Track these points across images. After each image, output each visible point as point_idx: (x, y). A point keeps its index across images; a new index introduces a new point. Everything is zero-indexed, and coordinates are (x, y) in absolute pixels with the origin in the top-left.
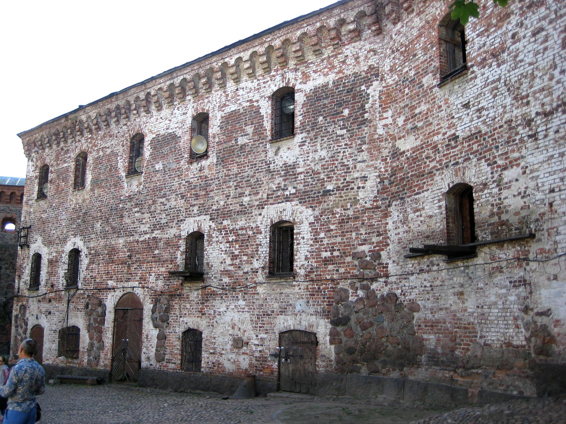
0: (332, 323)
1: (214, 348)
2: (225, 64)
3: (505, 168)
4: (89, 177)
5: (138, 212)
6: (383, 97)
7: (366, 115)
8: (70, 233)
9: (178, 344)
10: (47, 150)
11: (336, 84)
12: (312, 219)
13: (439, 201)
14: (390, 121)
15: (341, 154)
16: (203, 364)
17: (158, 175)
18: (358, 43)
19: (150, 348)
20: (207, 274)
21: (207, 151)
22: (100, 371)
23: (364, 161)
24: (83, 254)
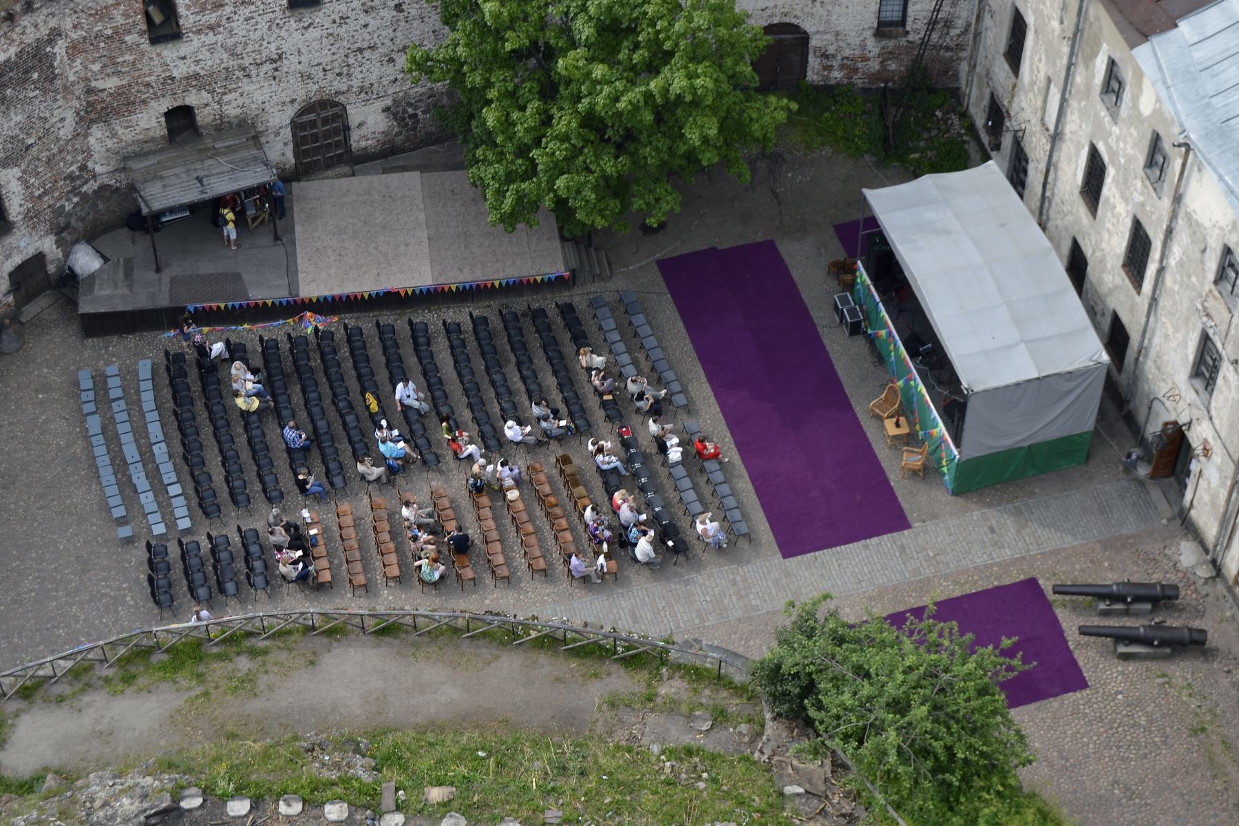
3: (225, 94)
7: (57, 72)
11: (19, 55)
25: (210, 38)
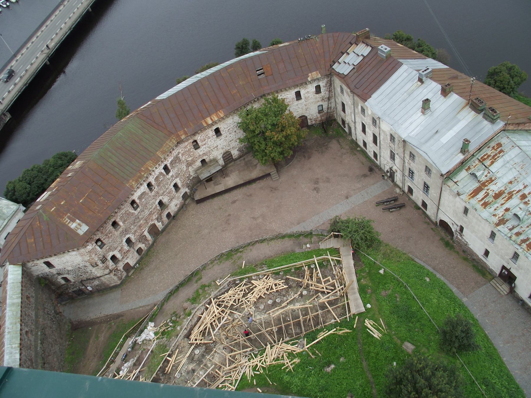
25: (205, 146)
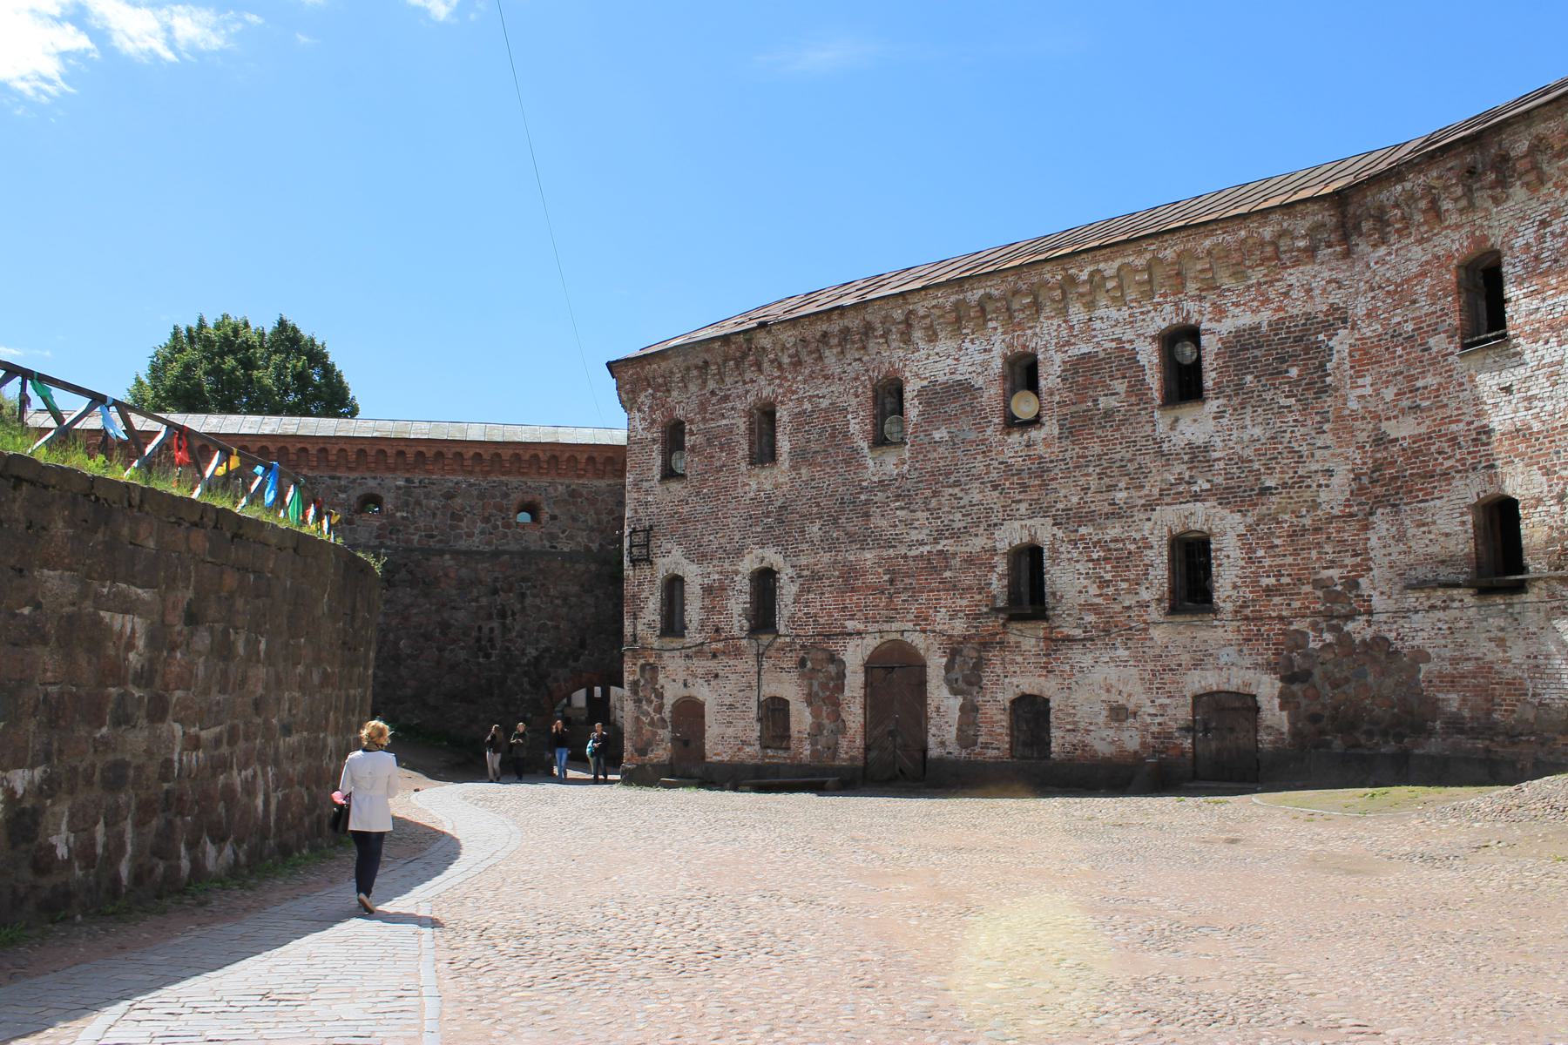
0: (1282, 679)
1: (1075, 723)
2: (1072, 281)
4: (784, 445)
5: (902, 508)
6: (1357, 355)
7: (1329, 380)
8: (749, 541)
9: (1003, 720)
10: (675, 393)
11: (1275, 326)
12: (1241, 529)
13: (1462, 514)
14: (1368, 391)
15: (1288, 435)
16: (1054, 747)
17: (940, 450)
18: (1309, 267)
19: (946, 727)
20: (1054, 609)
21: (1038, 416)
22: (843, 768)
23: (1327, 447)
24: (783, 578)
